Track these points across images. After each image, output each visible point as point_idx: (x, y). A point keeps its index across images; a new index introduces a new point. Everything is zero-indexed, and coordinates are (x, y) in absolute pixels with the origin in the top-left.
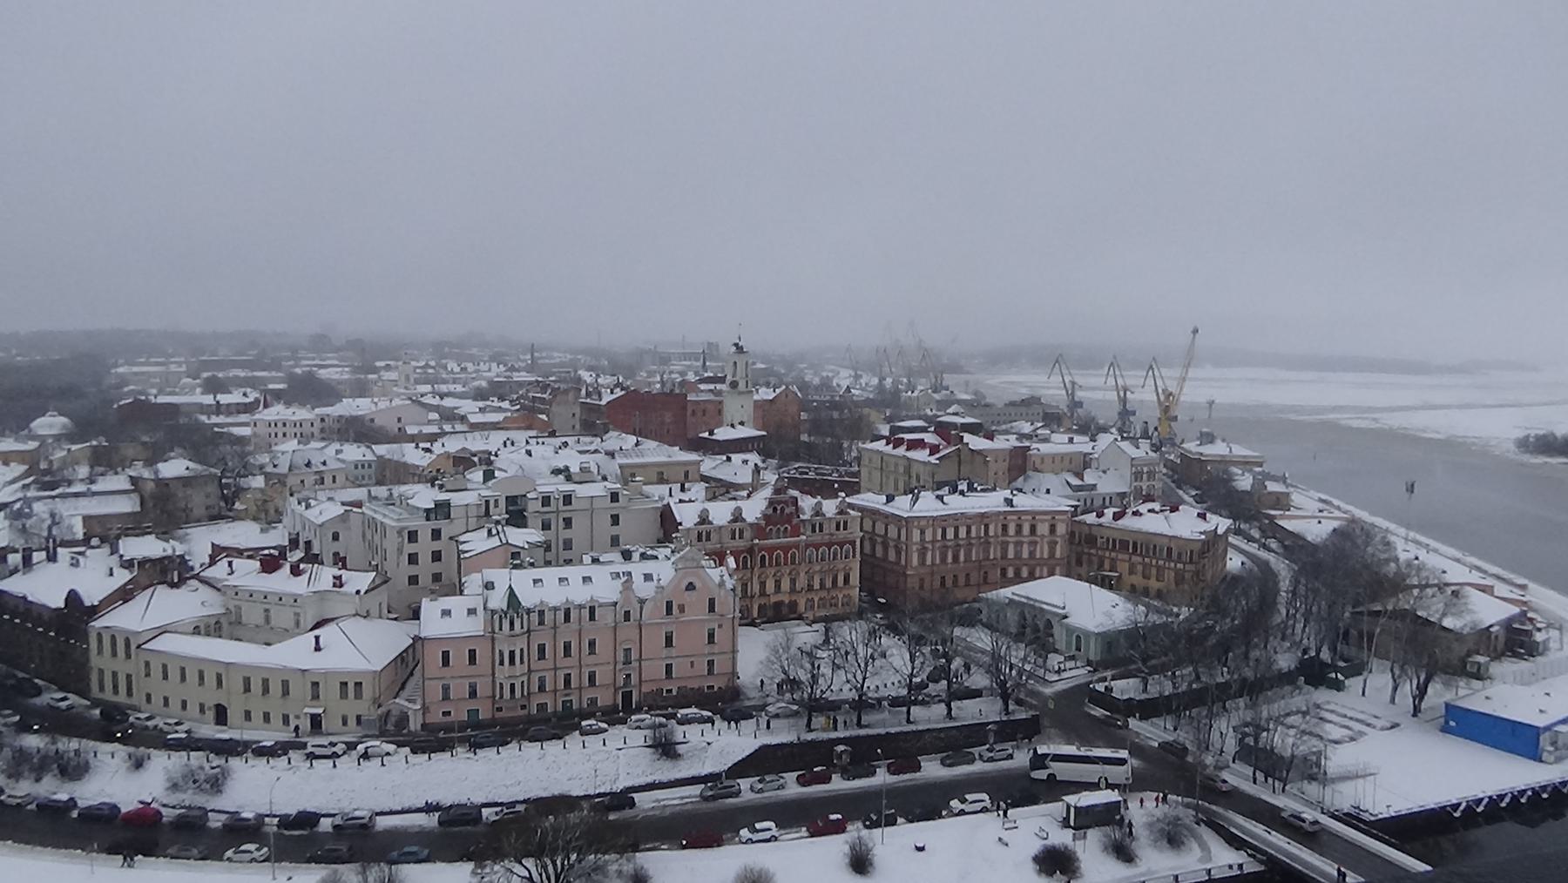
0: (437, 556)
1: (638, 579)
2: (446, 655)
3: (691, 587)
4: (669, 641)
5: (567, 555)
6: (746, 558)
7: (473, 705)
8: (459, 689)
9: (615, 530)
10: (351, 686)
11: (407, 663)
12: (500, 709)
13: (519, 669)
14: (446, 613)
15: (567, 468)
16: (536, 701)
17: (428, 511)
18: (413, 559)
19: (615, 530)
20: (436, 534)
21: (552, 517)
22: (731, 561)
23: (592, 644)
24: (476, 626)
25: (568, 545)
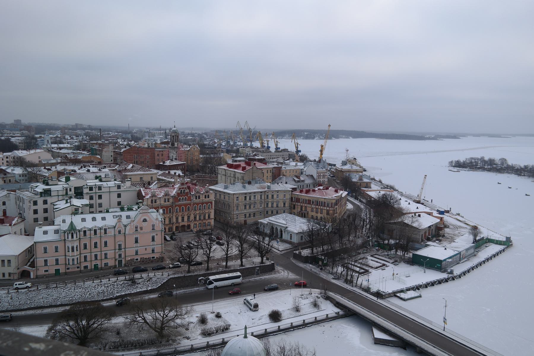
0: (46, 211)
1: (124, 219)
2: (45, 249)
3: (145, 220)
4: (136, 241)
5: (100, 209)
6: (167, 210)
7: (46, 268)
8: (51, 261)
9: (119, 200)
10: (6, 262)
11: (30, 251)
12: (68, 269)
13: (76, 253)
14: (45, 233)
15: (100, 176)
16: (83, 265)
17: (41, 192)
18: (36, 212)
19: (119, 200)
20: (45, 202)
21: (94, 195)
22: (161, 211)
23: (106, 243)
24: (56, 237)
25: (100, 205)
